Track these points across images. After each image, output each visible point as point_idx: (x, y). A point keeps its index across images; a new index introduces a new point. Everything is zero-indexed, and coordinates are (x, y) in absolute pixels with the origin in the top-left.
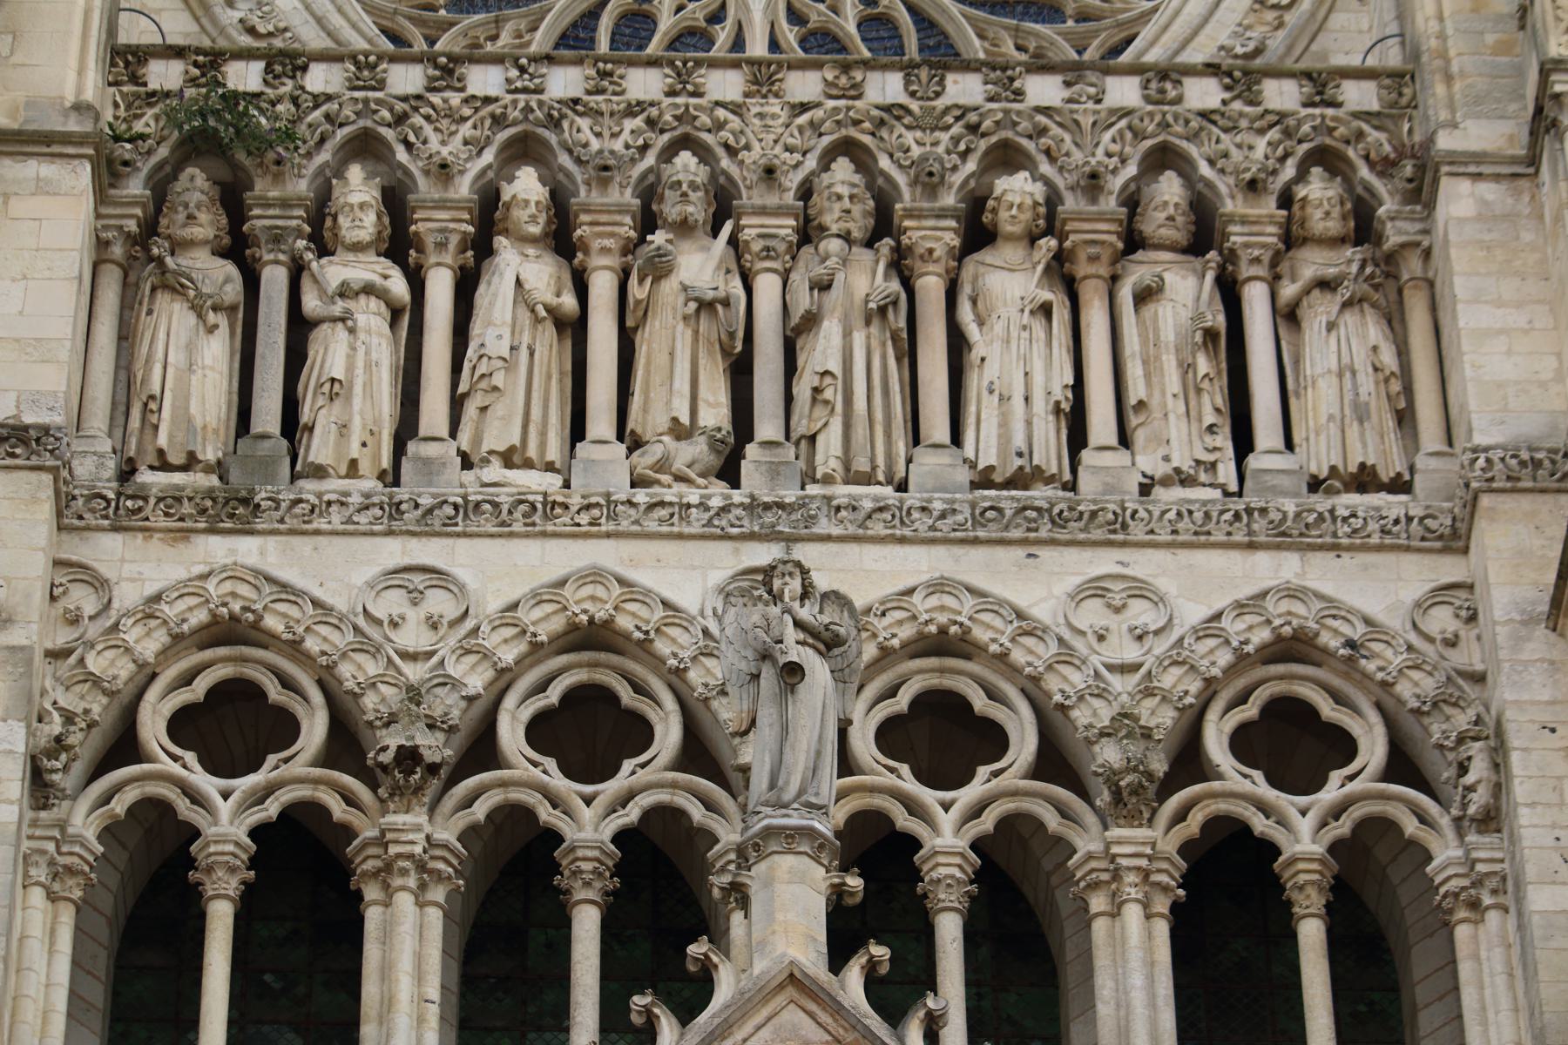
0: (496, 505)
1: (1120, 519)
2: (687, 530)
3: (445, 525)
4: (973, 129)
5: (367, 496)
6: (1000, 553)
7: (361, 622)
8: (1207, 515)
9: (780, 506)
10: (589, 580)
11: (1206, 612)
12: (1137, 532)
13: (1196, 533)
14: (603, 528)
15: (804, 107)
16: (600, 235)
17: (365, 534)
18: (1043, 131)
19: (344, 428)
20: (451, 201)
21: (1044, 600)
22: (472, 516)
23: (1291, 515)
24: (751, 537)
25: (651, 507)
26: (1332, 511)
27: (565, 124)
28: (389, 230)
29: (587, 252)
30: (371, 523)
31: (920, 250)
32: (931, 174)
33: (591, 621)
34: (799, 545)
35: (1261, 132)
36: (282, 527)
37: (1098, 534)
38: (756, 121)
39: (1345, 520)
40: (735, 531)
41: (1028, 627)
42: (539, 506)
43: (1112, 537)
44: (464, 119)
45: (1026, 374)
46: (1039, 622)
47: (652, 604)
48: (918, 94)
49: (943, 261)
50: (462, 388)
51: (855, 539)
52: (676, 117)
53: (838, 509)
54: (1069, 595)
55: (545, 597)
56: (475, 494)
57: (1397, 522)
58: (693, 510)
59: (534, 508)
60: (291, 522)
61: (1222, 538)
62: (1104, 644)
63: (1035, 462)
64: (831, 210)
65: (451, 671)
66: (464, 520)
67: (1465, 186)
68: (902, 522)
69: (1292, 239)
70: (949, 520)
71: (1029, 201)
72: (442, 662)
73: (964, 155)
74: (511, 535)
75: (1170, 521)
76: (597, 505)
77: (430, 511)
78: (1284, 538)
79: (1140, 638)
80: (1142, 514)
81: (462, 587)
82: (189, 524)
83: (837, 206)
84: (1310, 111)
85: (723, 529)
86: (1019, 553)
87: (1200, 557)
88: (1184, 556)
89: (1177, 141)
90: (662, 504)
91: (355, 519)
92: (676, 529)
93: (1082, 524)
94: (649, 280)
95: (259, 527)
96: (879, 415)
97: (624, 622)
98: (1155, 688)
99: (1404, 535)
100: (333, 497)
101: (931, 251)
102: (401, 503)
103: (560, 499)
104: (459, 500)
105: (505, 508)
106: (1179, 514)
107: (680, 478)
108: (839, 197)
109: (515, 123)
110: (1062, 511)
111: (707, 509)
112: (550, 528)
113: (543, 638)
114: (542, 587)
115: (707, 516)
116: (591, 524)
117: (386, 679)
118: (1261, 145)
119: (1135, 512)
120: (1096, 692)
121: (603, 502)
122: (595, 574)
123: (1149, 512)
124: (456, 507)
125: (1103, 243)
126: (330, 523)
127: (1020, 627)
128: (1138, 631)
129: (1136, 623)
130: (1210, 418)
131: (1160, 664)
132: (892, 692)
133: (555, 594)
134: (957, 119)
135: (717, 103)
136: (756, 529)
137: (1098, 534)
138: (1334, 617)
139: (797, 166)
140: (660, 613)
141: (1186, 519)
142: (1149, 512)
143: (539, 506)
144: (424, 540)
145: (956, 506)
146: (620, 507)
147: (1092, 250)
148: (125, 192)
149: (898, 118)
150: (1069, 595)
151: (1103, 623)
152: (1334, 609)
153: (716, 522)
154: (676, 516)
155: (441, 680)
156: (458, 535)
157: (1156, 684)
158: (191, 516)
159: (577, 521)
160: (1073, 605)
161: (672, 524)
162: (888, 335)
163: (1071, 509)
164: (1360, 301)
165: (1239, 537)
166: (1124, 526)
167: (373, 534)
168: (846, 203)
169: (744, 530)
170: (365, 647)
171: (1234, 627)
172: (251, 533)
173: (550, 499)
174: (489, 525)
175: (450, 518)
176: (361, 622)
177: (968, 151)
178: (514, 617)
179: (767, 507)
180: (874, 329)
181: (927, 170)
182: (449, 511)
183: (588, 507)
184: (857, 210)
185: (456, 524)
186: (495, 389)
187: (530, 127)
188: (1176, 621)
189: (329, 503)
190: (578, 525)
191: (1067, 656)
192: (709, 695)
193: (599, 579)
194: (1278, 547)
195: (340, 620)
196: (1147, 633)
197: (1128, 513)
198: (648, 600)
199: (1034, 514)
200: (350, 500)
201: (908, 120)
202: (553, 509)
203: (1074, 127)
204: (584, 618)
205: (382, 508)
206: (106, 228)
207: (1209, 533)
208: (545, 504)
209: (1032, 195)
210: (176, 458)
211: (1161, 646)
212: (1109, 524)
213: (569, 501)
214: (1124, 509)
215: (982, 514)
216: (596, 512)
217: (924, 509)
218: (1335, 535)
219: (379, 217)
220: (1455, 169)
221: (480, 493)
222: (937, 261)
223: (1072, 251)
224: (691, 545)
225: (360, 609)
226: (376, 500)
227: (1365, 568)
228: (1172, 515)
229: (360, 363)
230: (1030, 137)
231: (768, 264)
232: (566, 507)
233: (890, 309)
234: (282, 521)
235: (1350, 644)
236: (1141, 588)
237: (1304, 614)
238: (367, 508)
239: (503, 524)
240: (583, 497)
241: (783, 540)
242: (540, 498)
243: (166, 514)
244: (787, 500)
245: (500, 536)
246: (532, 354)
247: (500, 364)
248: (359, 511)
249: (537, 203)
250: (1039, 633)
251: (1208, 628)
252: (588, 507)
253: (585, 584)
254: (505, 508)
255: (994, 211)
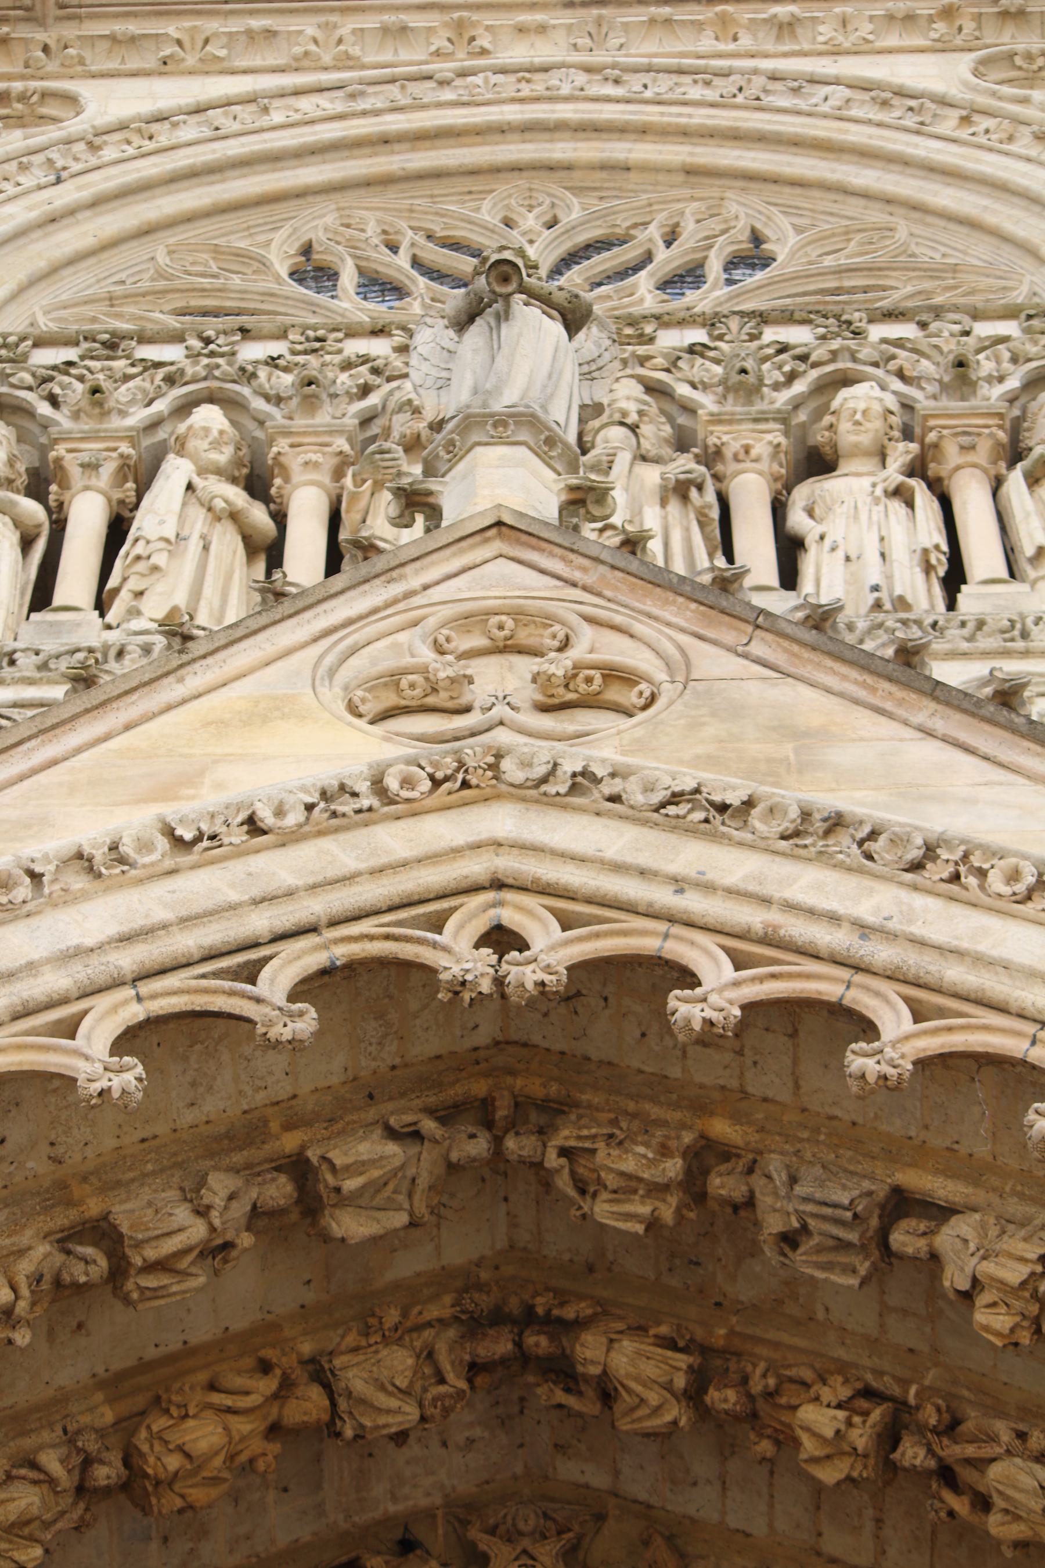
20: (106, 431)
28: (25, 477)
29: (287, 480)
31: (728, 453)
32: (744, 371)
45: (882, 539)
48: (727, 338)
50: (112, 583)
63: (898, 591)
93: (966, 632)
94: (369, 483)
101: (747, 450)
109: (194, 380)
162: (692, 516)
166: (1025, 635)
181: (738, 366)
186: (155, 569)
187: (215, 384)
203: (934, 353)
209: (881, 400)
212: (1004, 632)
222: (756, 460)
223: (936, 446)
230: (876, 365)
246: (206, 548)
247: (162, 545)
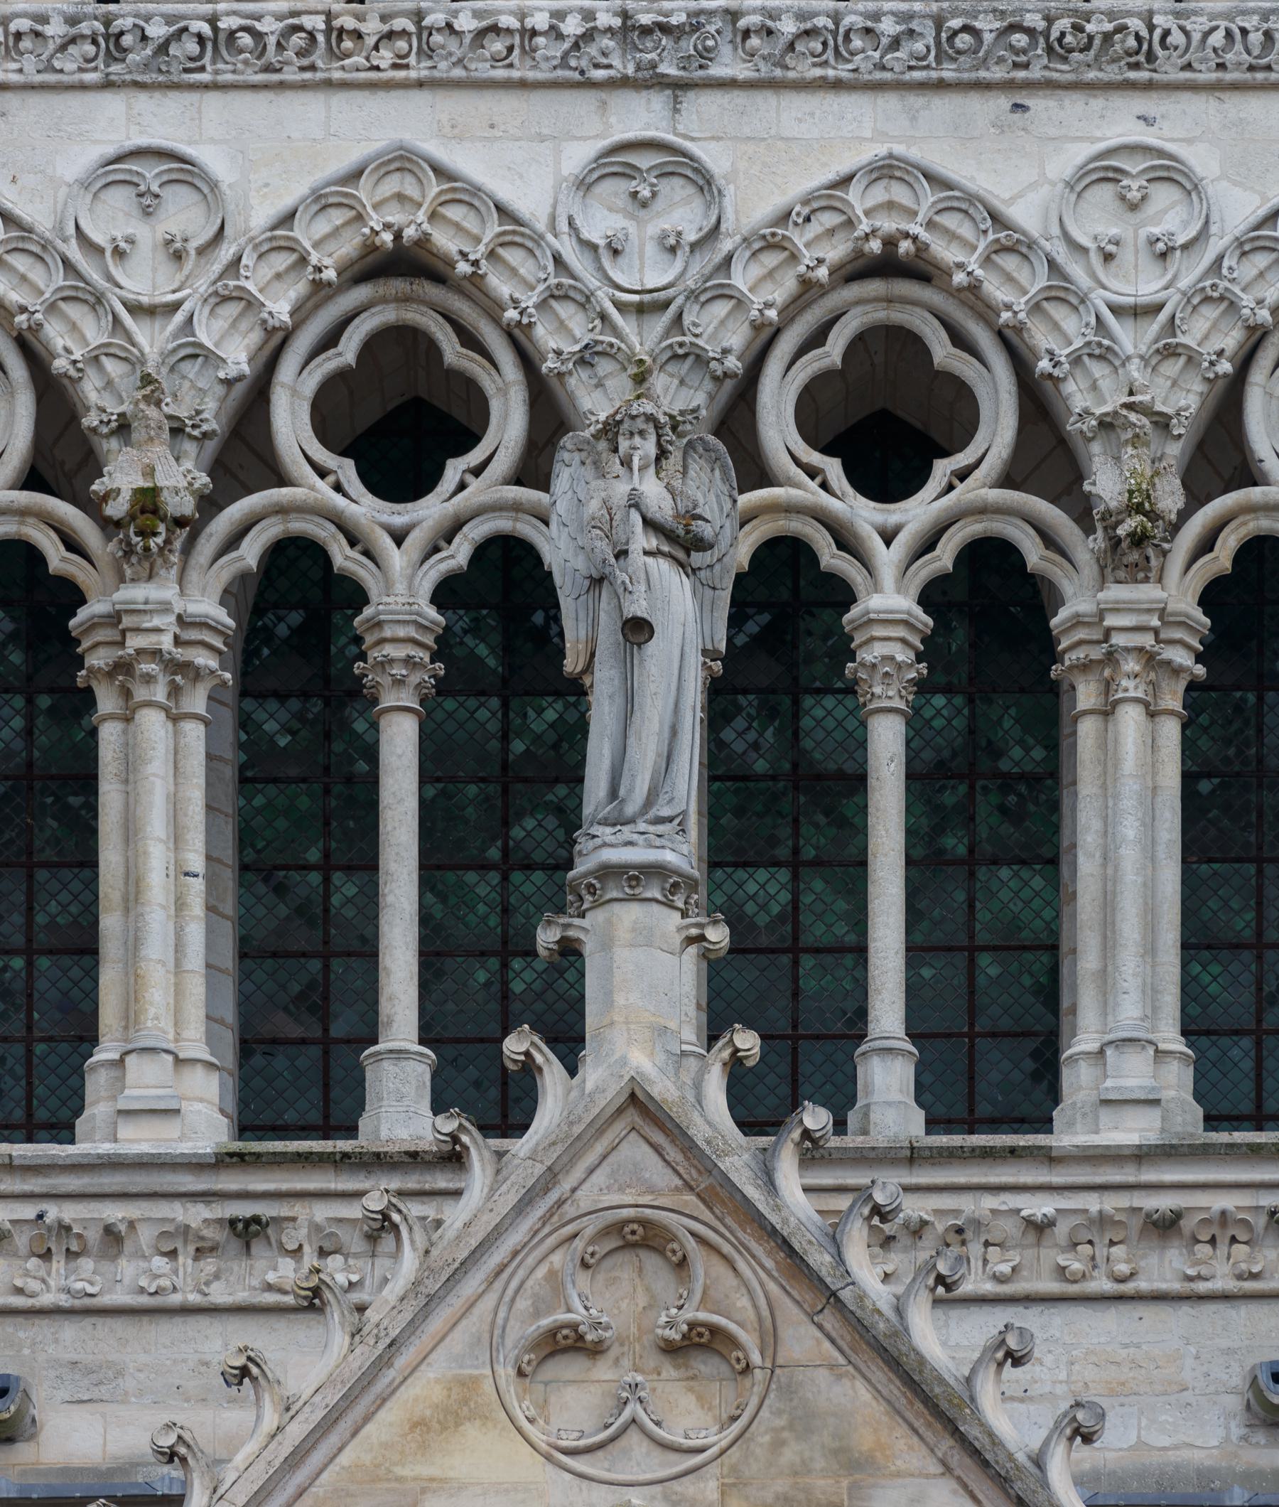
0: (257, 36)
1: (1145, 47)
2: (531, 75)
3: (186, 70)
5: (72, 21)
7: (74, 252)
9: (665, 29)
10: (392, 167)
13: (1251, 68)
14: (413, 74)
21: (1032, 186)
22: (224, 53)
25: (481, 34)
30: (81, 70)
33: (398, 236)
34: (691, 95)
37: (1112, 73)
40: (600, 74)
42: (321, 38)
43: (1132, 75)
46: (1024, 233)
47: (483, 209)
53: (746, 34)
54: (1067, 183)
55: (332, 200)
56: (228, 14)
58: (541, 41)
59: (311, 35)
65: (203, 337)
66: (214, 62)
72: (190, 320)
74: (282, 86)
75: (1215, 50)
76: (404, 33)
77: (163, 48)
80: (1177, 38)
81: (214, 185)
85: (582, 72)
91: (57, 65)
92: (515, 74)
97: (445, 241)
98: (1178, 345)
100: (23, 24)
102: (122, 33)
103: (349, 23)
104: (206, 29)
105: (272, 41)
106: (1229, 34)
110: (1063, 34)
111: (560, 36)
112: (337, 75)
113: (330, 274)
114: (328, 184)
116: (395, 66)
117: (112, 351)
119: (1166, 33)
120: (1097, 352)
121: (411, 28)
122: (401, 157)
124: (201, 39)
126: (20, 71)
127: (997, 241)
128: (1161, 246)
129: (1157, 231)
131: (1189, 301)
133: (346, 195)
136: (630, 70)
140: (493, 228)
141: (1239, 46)
143: (321, 38)
144: (157, 95)
145: (914, 25)
146: (437, 38)
150: (1067, 183)
151: (1114, 231)
153: (573, 63)
154: (516, 52)
155: (189, 351)
156: (206, 87)
157: (1181, 339)
159: (375, 63)
160: (1073, 197)
161: (511, 66)
163: (1078, 28)
166: (1151, 57)
169: (612, 72)
170: (80, 295)
173: (337, 23)
174: (249, 71)
175: (191, 59)
176: (74, 252)
178: (288, 238)
179: (646, 31)
182: (192, 47)
183: (390, 35)
185: (202, 69)
188: (1214, 229)
189: (18, 36)
190: (377, 68)
192: (564, 369)
193: (408, 165)
195: (44, 247)
196: (1173, 248)
197: (1157, 33)
198: (476, 203)
200: (49, 30)
202: (340, 39)
204: (387, 237)
205: (95, 42)
207: (1268, 68)
208: (329, 30)
211: (1190, 272)
213: (364, 28)
214: (1151, 28)
215: (951, 38)
216: (402, 45)
217: (868, 31)
221: (235, 13)
224: (538, 97)
225: (71, 230)
226: (85, 28)
228: (1217, 39)
232: (358, 35)
236: (1168, 168)
238: (73, 40)
239: (268, 69)
240: (384, 18)
242: (318, 23)
244: (674, 21)
245: (266, 86)
248: (63, 48)
250: (1024, 250)
251: (1258, 238)
252: (390, 35)
253: (388, 173)
254: (272, 41)
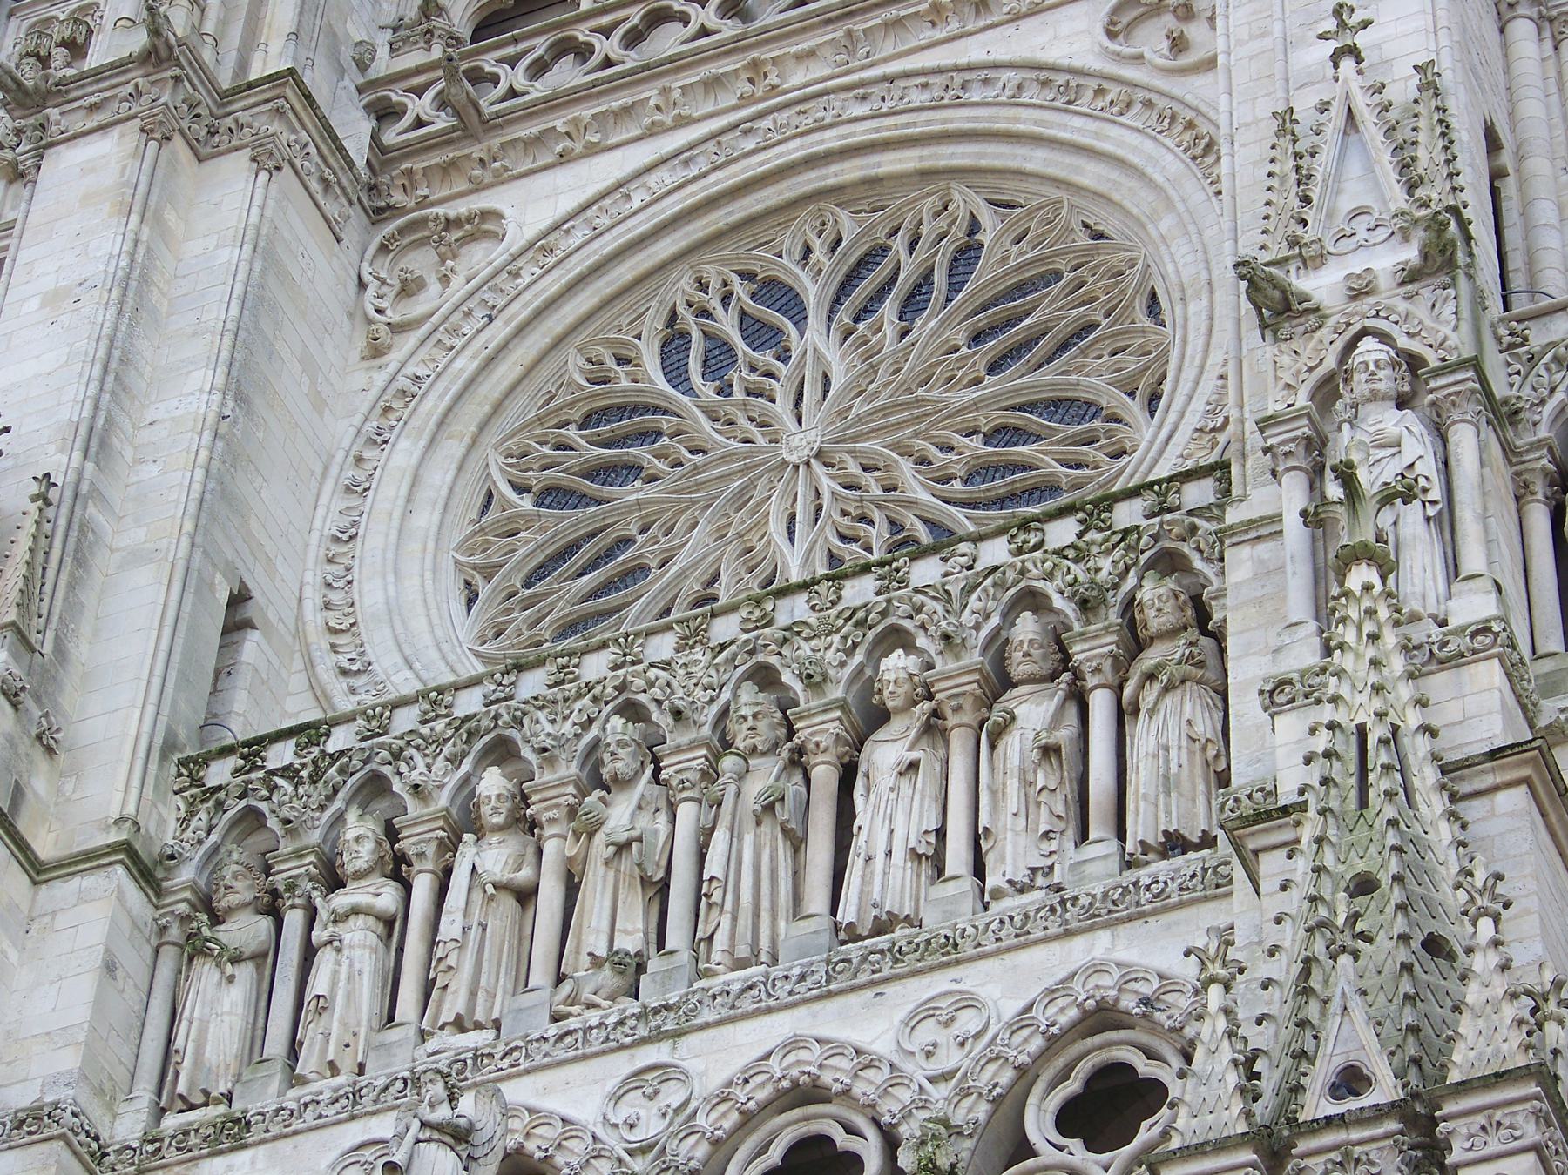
2: (588, 1050)
4: (860, 624)
6: (853, 999)
8: (1026, 916)
9: (667, 1007)
11: (1021, 1004)
12: (968, 949)
13: (1017, 936)
15: (723, 647)
16: (547, 809)
17: (333, 1124)
18: (919, 609)
19: (327, 1036)
23: (1099, 896)
24: (644, 1041)
25: (561, 1038)
26: (1135, 884)
27: (526, 721)
35: (1108, 552)
36: (267, 1135)
37: (930, 960)
38: (682, 672)
39: (1148, 888)
40: (628, 1040)
41: (865, 1060)
44: (446, 741)
49: (832, 750)
50: (432, 976)
51: (732, 1020)
52: (615, 688)
53: (714, 997)
57: (1193, 876)
60: (276, 1130)
61: (1040, 934)
62: (932, 1059)
64: (740, 731)
67: (1245, 551)
68: (769, 995)
69: (1135, 640)
70: (809, 982)
71: (903, 675)
73: (850, 652)
76: (517, 1048)
78: (1097, 918)
79: (962, 1044)
82: (196, 1153)
83: (745, 726)
84: (1151, 521)
86: (869, 994)
87: (1023, 956)
88: (1009, 959)
89: (1035, 583)
90: (569, 1033)
92: (580, 1052)
95: (250, 1140)
96: (765, 904)
99: (1200, 887)
104: (407, 1074)
106: (1002, 922)
107: (591, 1006)
108: (745, 718)
109: (488, 732)
115: (604, 1034)
116: (512, 1066)
118: (1106, 564)
123: (976, 927)
125: (964, 694)
130: (1043, 828)
132: (764, 1149)
134: (847, 620)
135: (652, 665)
137: (930, 960)
138: (1136, 980)
139: (712, 700)
142: (976, 927)
144: (381, 1116)
147: (954, 703)
148: (177, 880)
149: (798, 633)
152: (1130, 975)
158: (196, 1145)
164: (1183, 682)
165: (1053, 930)
166: (956, 945)
167: (339, 1122)
168: (750, 722)
171: (1040, 1016)
172: (245, 1147)
177: (855, 645)
180: (765, 828)
184: (762, 725)
186: (450, 968)
191: (898, 1077)
194: (1091, 929)
199: (878, 956)
200: (320, 1098)
201: (806, 632)
206: (162, 916)
210: (198, 1099)
218: (1138, 904)
219: (379, 843)
220: (1234, 540)
227: (1168, 927)
228: (994, 926)
229: (343, 976)
231: (685, 794)
233: (778, 806)
234: (267, 1131)
235: (1145, 1001)
237: (1107, 984)
238: (337, 1101)
241: (667, 1038)
243: (178, 1149)
247: (452, 945)
249: (499, 796)
255: (880, 692)
